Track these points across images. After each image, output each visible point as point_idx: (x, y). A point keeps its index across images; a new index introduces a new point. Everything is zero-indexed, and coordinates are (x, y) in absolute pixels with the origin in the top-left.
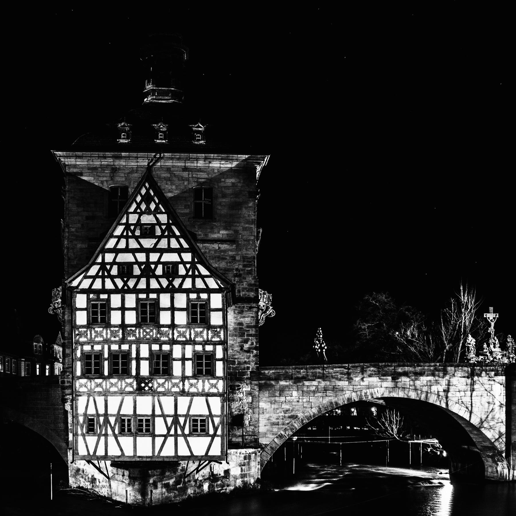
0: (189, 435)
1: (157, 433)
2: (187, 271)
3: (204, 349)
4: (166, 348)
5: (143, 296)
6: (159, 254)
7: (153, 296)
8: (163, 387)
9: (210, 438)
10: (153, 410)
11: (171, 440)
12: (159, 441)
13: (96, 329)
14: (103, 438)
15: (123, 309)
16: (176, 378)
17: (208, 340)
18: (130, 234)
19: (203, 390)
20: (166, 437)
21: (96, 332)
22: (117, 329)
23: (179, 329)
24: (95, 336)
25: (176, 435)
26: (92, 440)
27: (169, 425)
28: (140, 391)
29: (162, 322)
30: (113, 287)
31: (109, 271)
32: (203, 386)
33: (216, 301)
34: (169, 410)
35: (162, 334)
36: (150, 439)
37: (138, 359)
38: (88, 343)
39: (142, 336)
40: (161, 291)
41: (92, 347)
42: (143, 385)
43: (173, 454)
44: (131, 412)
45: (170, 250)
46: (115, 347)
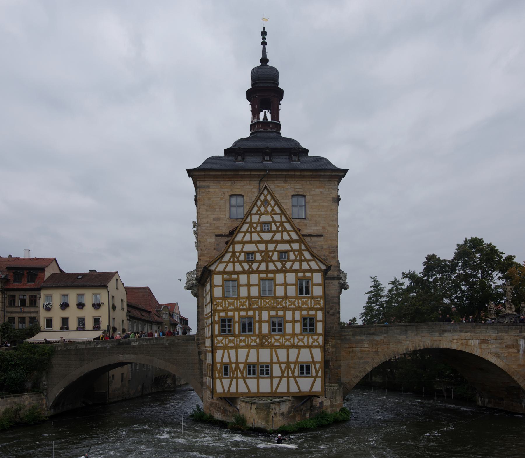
1: (274, 375)
2: (296, 256)
3: (308, 313)
4: (281, 313)
5: (263, 275)
6: (275, 245)
7: (271, 275)
8: (279, 342)
9: (313, 379)
10: (272, 359)
11: (284, 380)
12: (276, 381)
13: (229, 300)
14: (234, 380)
16: (288, 335)
17: (311, 308)
18: (253, 230)
19: (308, 343)
20: (281, 378)
21: (229, 302)
22: (244, 300)
23: (290, 300)
24: (229, 306)
25: (288, 377)
27: (283, 369)
28: (262, 345)
29: (277, 295)
30: (241, 270)
31: (238, 258)
32: (308, 340)
33: (318, 278)
34: (283, 357)
35: (278, 303)
36: (269, 380)
37: (260, 322)
38: (223, 311)
39: (263, 305)
40: (277, 271)
41: (226, 313)
42: (264, 341)
43: (285, 390)
45: (283, 241)
46: (243, 313)
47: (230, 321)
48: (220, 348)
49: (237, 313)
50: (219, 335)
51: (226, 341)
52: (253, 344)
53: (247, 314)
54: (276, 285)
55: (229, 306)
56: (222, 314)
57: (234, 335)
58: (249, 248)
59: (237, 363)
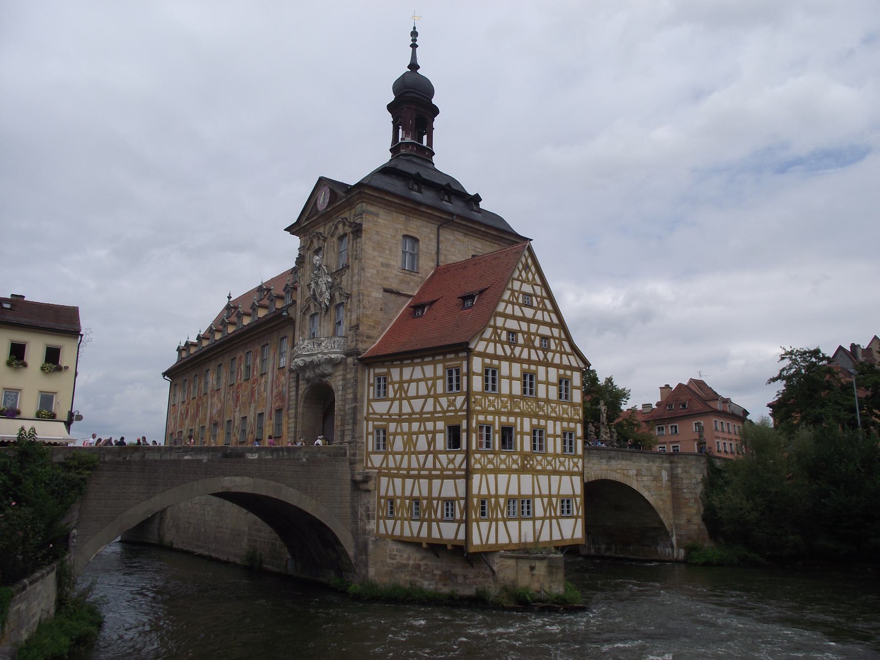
0: (562, 517)
2: (557, 346)
4: (542, 422)
7: (533, 367)
8: (541, 465)
10: (533, 491)
12: (538, 523)
14: (494, 523)
15: (510, 378)
16: (550, 455)
21: (489, 401)
24: (489, 406)
26: (484, 525)
28: (523, 470)
31: (499, 336)
36: (531, 522)
37: (522, 433)
40: (539, 363)
41: (486, 417)
44: (517, 493)
45: (544, 323)
46: (504, 419)
47: (488, 429)
48: (477, 471)
49: (497, 417)
50: (477, 451)
51: (484, 460)
52: (515, 466)
53: (508, 419)
54: (539, 382)
55: (489, 406)
56: (481, 418)
57: (493, 452)
58: (512, 324)
59: (497, 496)
